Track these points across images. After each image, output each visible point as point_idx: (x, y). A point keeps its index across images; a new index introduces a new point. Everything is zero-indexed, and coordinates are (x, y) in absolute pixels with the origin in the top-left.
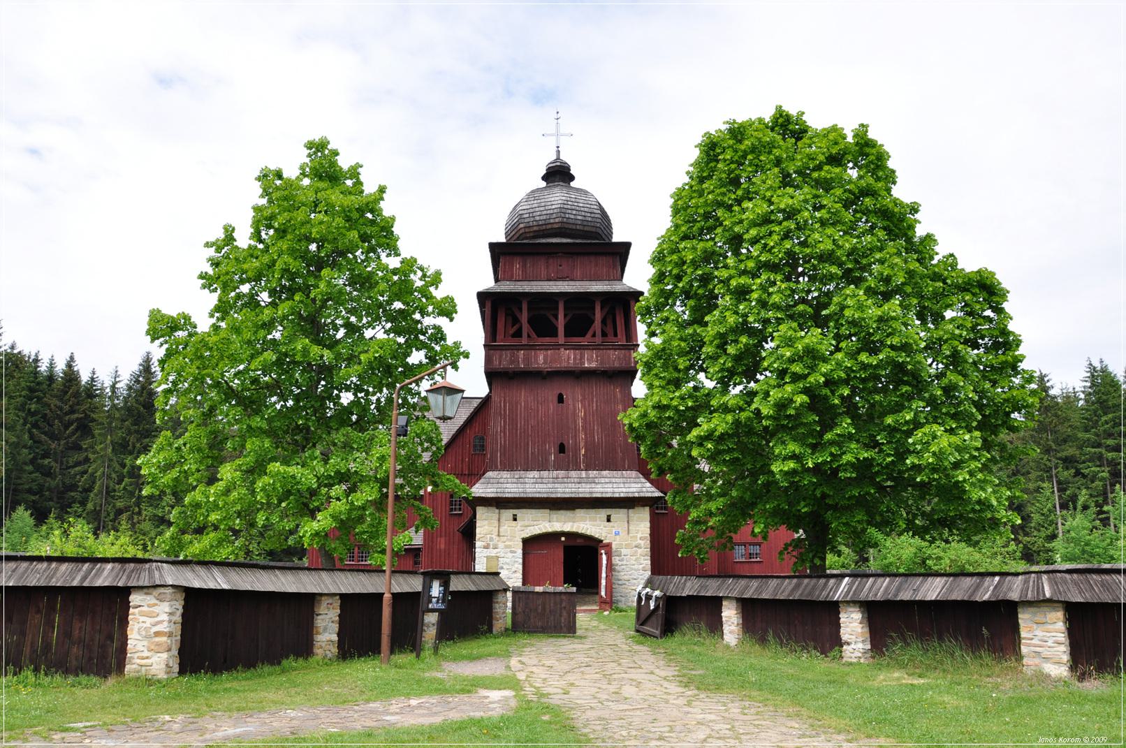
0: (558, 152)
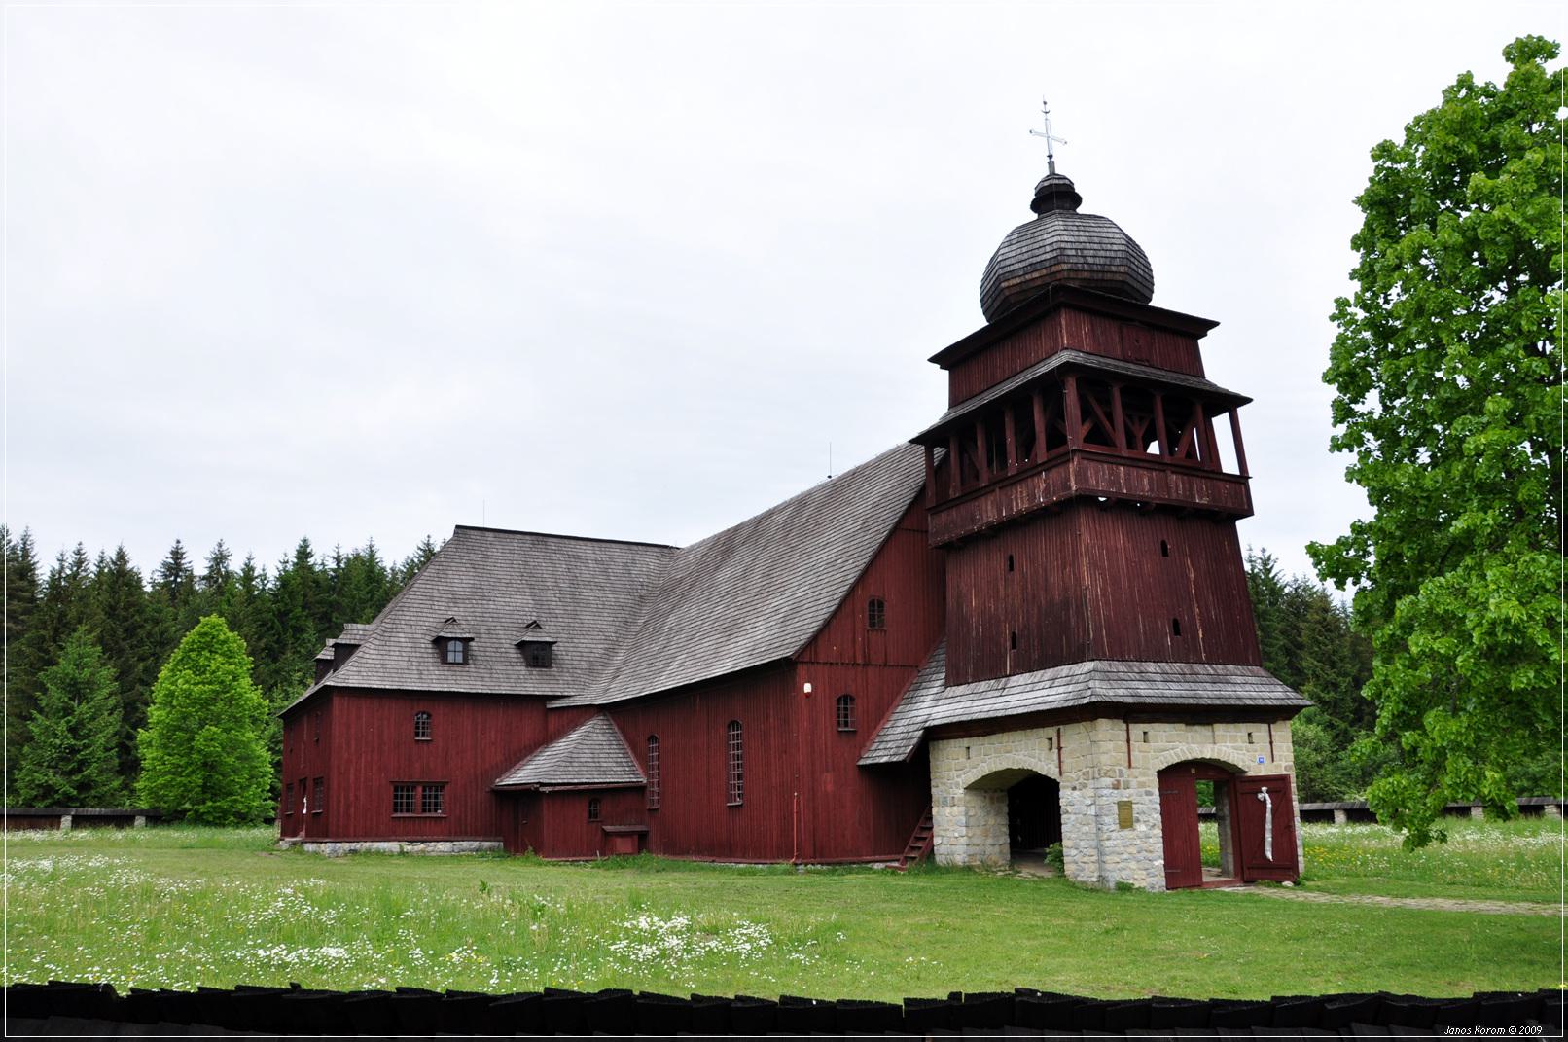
0: (1051, 164)
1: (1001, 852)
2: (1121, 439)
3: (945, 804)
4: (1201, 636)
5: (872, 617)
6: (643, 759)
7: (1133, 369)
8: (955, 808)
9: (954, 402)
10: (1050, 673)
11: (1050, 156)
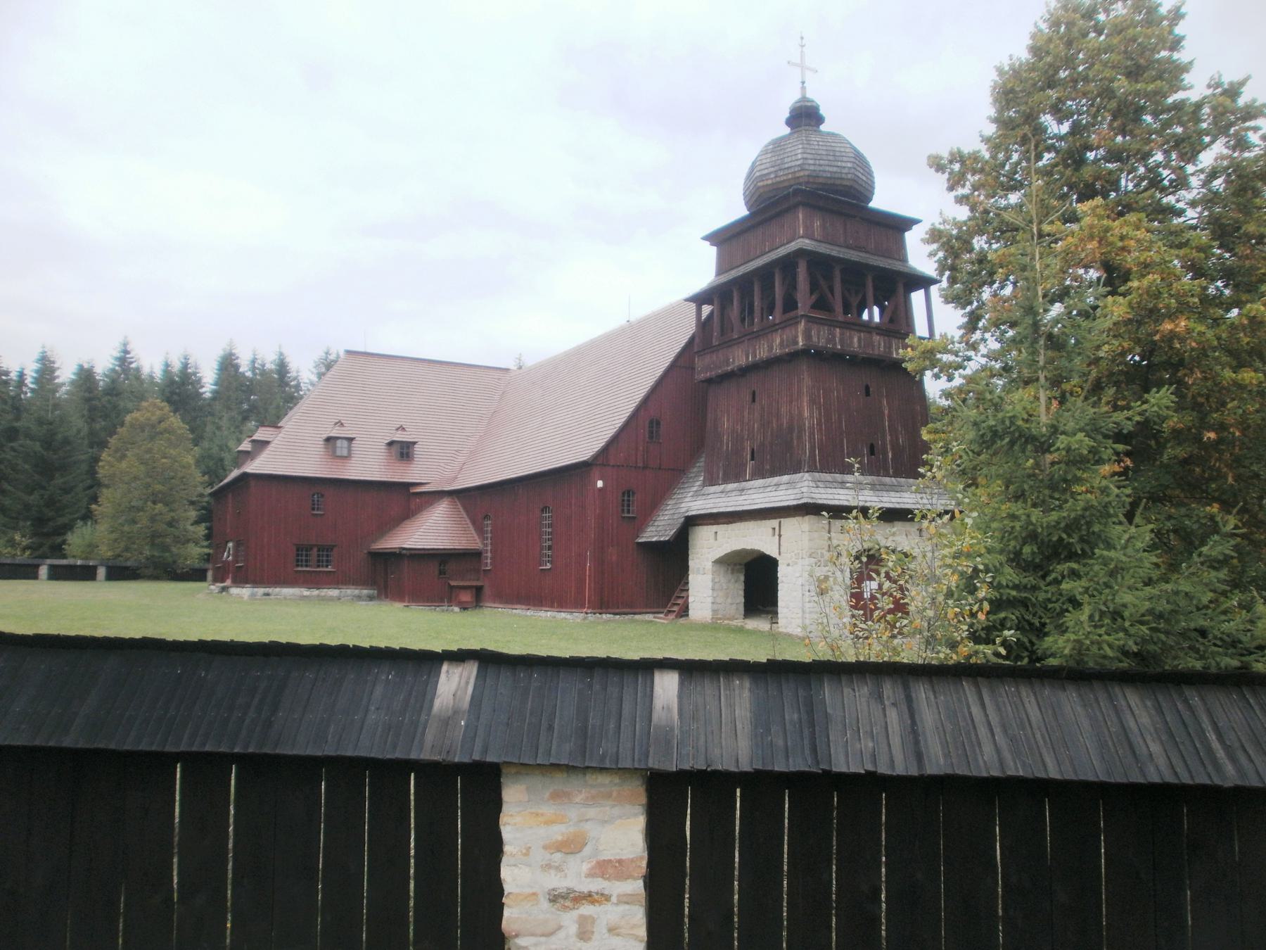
0: (803, 88)
1: (737, 609)
2: (839, 308)
4: (890, 456)
5: (651, 432)
6: (480, 530)
7: (854, 256)
9: (720, 272)
10: (776, 479)
11: (803, 83)
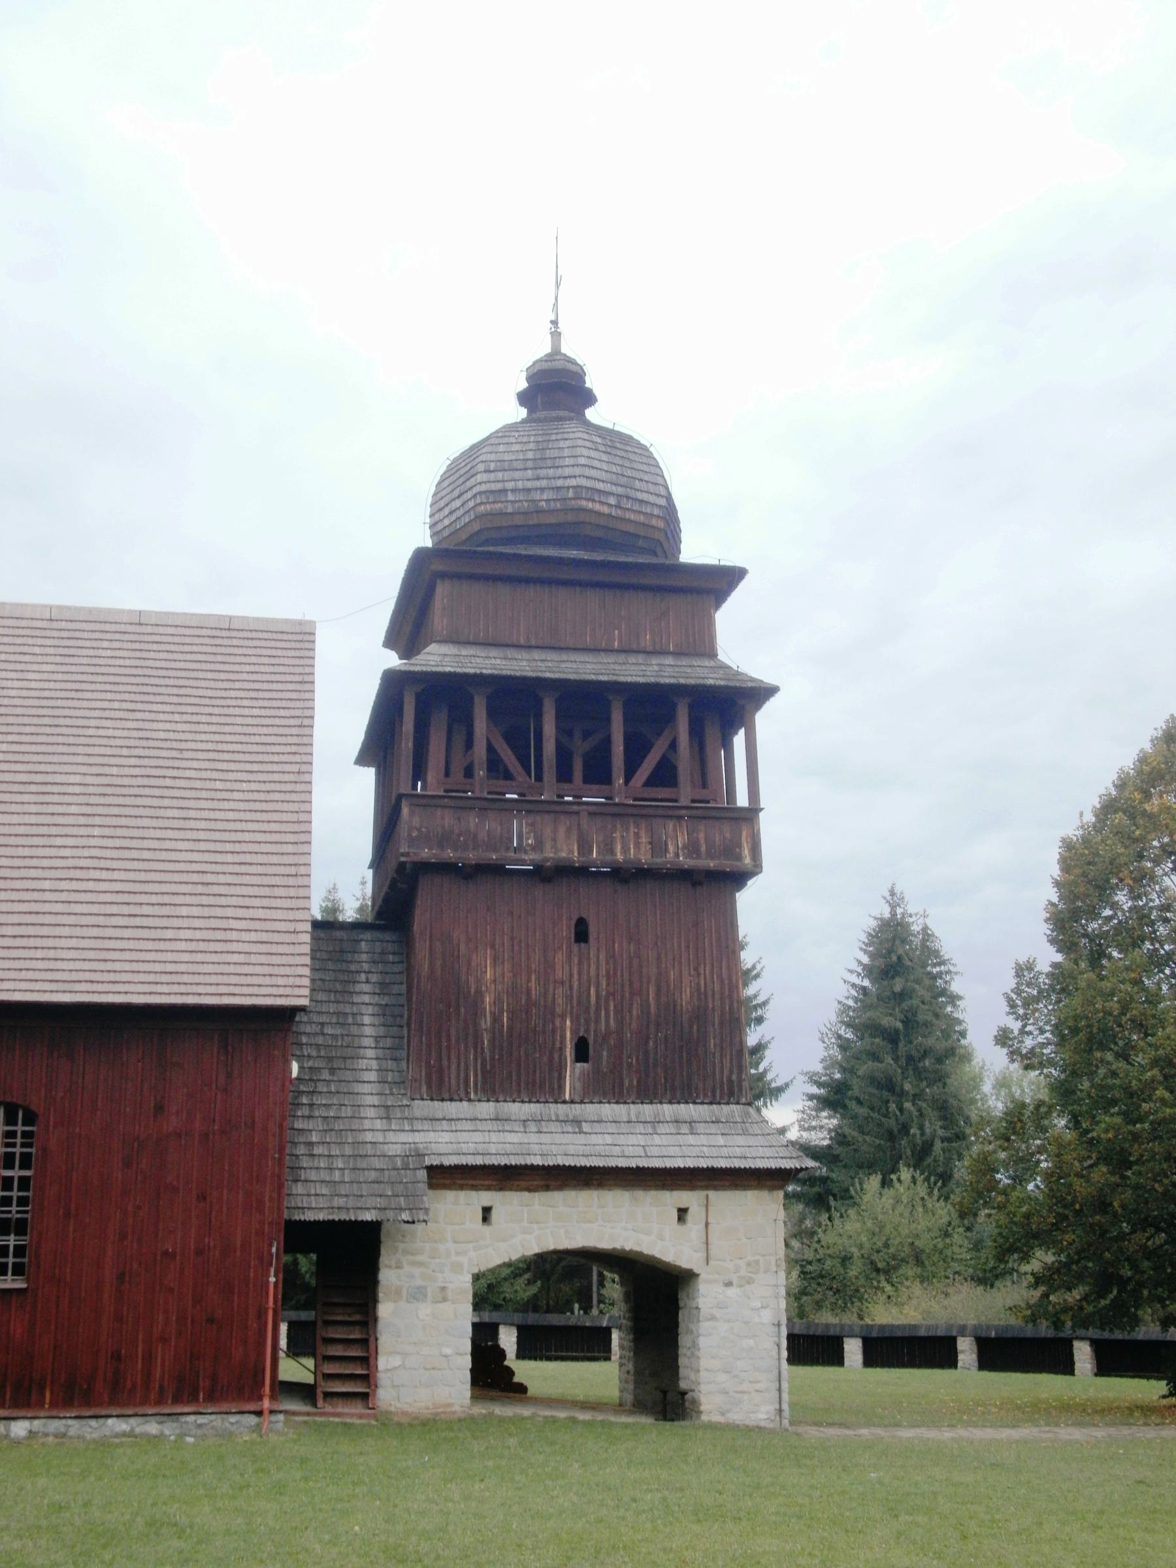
0: (556, 335)
3: (418, 1295)
8: (446, 1307)
11: (555, 323)
